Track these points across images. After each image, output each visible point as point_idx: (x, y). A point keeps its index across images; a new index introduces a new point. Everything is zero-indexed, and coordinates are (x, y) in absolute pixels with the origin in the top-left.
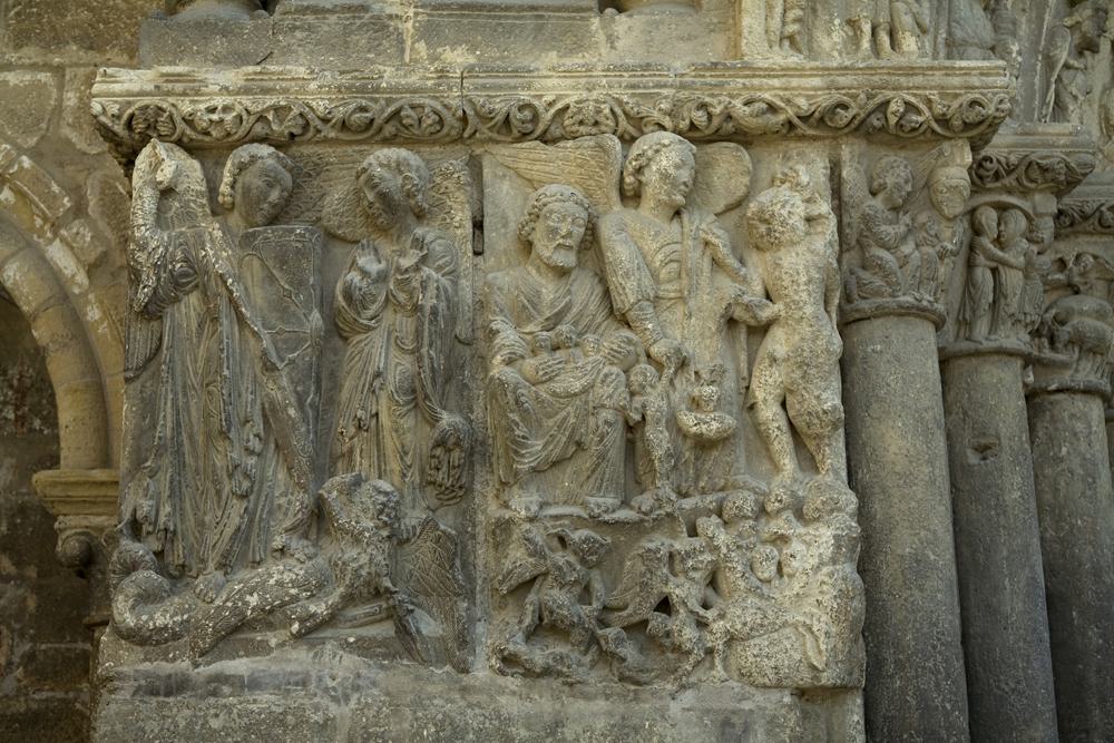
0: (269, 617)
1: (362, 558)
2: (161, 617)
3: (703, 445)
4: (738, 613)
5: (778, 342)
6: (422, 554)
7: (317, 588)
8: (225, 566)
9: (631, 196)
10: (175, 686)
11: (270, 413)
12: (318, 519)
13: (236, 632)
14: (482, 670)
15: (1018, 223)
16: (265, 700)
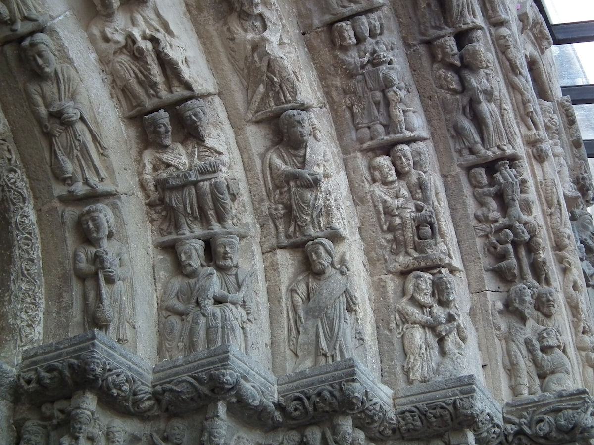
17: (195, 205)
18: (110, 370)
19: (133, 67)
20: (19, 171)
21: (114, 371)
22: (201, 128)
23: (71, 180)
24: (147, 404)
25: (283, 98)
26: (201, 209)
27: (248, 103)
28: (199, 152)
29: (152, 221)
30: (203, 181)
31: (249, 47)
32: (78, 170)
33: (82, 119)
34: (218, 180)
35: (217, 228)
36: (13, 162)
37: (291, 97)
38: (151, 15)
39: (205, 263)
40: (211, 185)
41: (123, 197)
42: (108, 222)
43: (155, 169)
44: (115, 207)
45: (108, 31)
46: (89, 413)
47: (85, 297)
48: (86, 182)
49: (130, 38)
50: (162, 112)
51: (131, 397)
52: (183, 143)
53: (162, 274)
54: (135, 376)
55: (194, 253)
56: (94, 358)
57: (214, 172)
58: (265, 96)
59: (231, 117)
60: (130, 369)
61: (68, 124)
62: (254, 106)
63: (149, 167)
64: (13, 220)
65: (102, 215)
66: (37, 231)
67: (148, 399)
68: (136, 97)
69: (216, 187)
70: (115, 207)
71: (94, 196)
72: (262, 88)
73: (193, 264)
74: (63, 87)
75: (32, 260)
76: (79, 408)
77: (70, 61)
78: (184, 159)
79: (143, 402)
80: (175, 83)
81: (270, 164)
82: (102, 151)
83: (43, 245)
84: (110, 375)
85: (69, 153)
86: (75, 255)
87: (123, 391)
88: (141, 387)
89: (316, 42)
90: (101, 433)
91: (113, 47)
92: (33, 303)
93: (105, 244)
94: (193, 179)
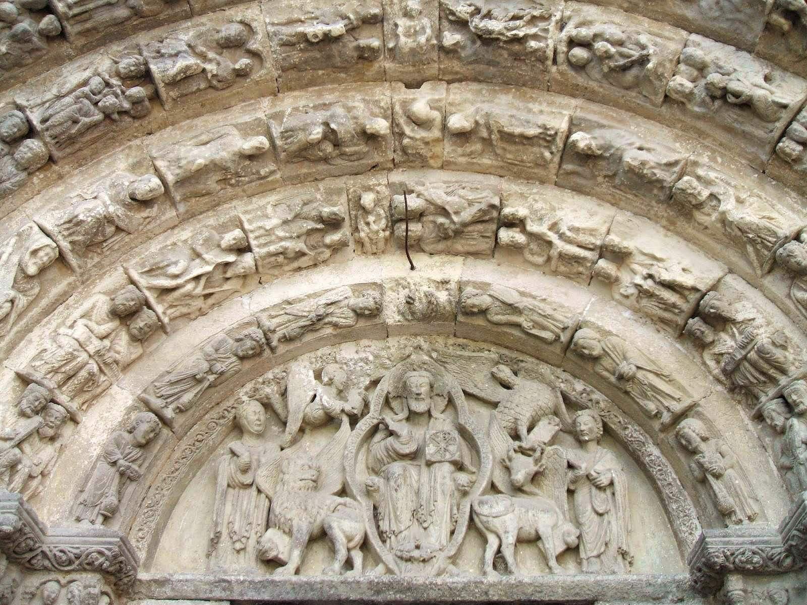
17: (757, 375)
18: (732, 554)
19: (653, 303)
20: (630, 426)
21: (737, 553)
22: (723, 313)
23: (658, 415)
24: (788, 561)
25: (769, 244)
26: (763, 373)
27: (750, 263)
28: (738, 329)
29: (739, 402)
30: (749, 352)
31: (719, 225)
32: (659, 404)
33: (638, 368)
34: (759, 344)
35: (783, 380)
36: (622, 422)
37: (774, 237)
38: (641, 258)
39: (788, 416)
40: (756, 352)
41: (702, 402)
42: (694, 432)
43: (718, 362)
44: (699, 415)
45: (622, 291)
46: (741, 592)
47: (710, 495)
48: (668, 410)
49: (637, 286)
50: (691, 321)
51: (770, 563)
52: (724, 330)
53: (768, 440)
54: (761, 546)
55: (774, 414)
56: (711, 553)
57: (752, 340)
58: (757, 252)
59: (750, 281)
60: (752, 543)
61: (632, 379)
62: (756, 263)
63: (712, 364)
64: (645, 462)
65: (686, 430)
66: (664, 460)
67: (787, 557)
68: (671, 321)
69: (761, 352)
70: (699, 415)
71: (679, 417)
72: (750, 249)
73: (777, 423)
74: (613, 356)
75: (670, 484)
76: (728, 592)
77: (609, 333)
78: (730, 343)
79: (783, 561)
80: (687, 293)
81: (797, 300)
82: (667, 379)
83: (674, 468)
84: (735, 558)
85: (645, 396)
86: (690, 467)
87: (756, 563)
88: (774, 551)
89: (776, 172)
90: (761, 601)
91: (633, 298)
92: (686, 516)
93: (703, 446)
94: (739, 357)
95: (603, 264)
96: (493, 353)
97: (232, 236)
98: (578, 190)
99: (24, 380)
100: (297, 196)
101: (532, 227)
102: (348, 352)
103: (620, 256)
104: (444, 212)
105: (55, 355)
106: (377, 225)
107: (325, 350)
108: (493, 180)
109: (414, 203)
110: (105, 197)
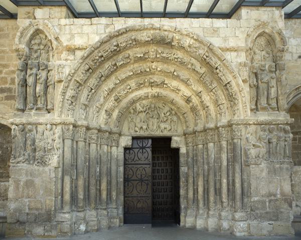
0: (20, 161)
1: (27, 157)
2: (13, 161)
3: (50, 149)
4: (50, 162)
5: (56, 141)
6: (31, 157)
7: (24, 159)
8: (18, 157)
9: (47, 130)
10: (14, 166)
11: (21, 147)
12: (24, 155)
13: (18, 162)
14: (34, 165)
15: (82, 130)
16: (20, 167)
71: (184, 114)
95: (177, 91)
96: (162, 102)
97: (129, 87)
98: (175, 80)
99: (106, 111)
100: (137, 79)
101: (168, 85)
102: (144, 102)
103: (179, 90)
104: (156, 82)
105: (109, 107)
106: (147, 84)
107: (141, 102)
108: (163, 77)
109: (152, 81)
110: (113, 84)
